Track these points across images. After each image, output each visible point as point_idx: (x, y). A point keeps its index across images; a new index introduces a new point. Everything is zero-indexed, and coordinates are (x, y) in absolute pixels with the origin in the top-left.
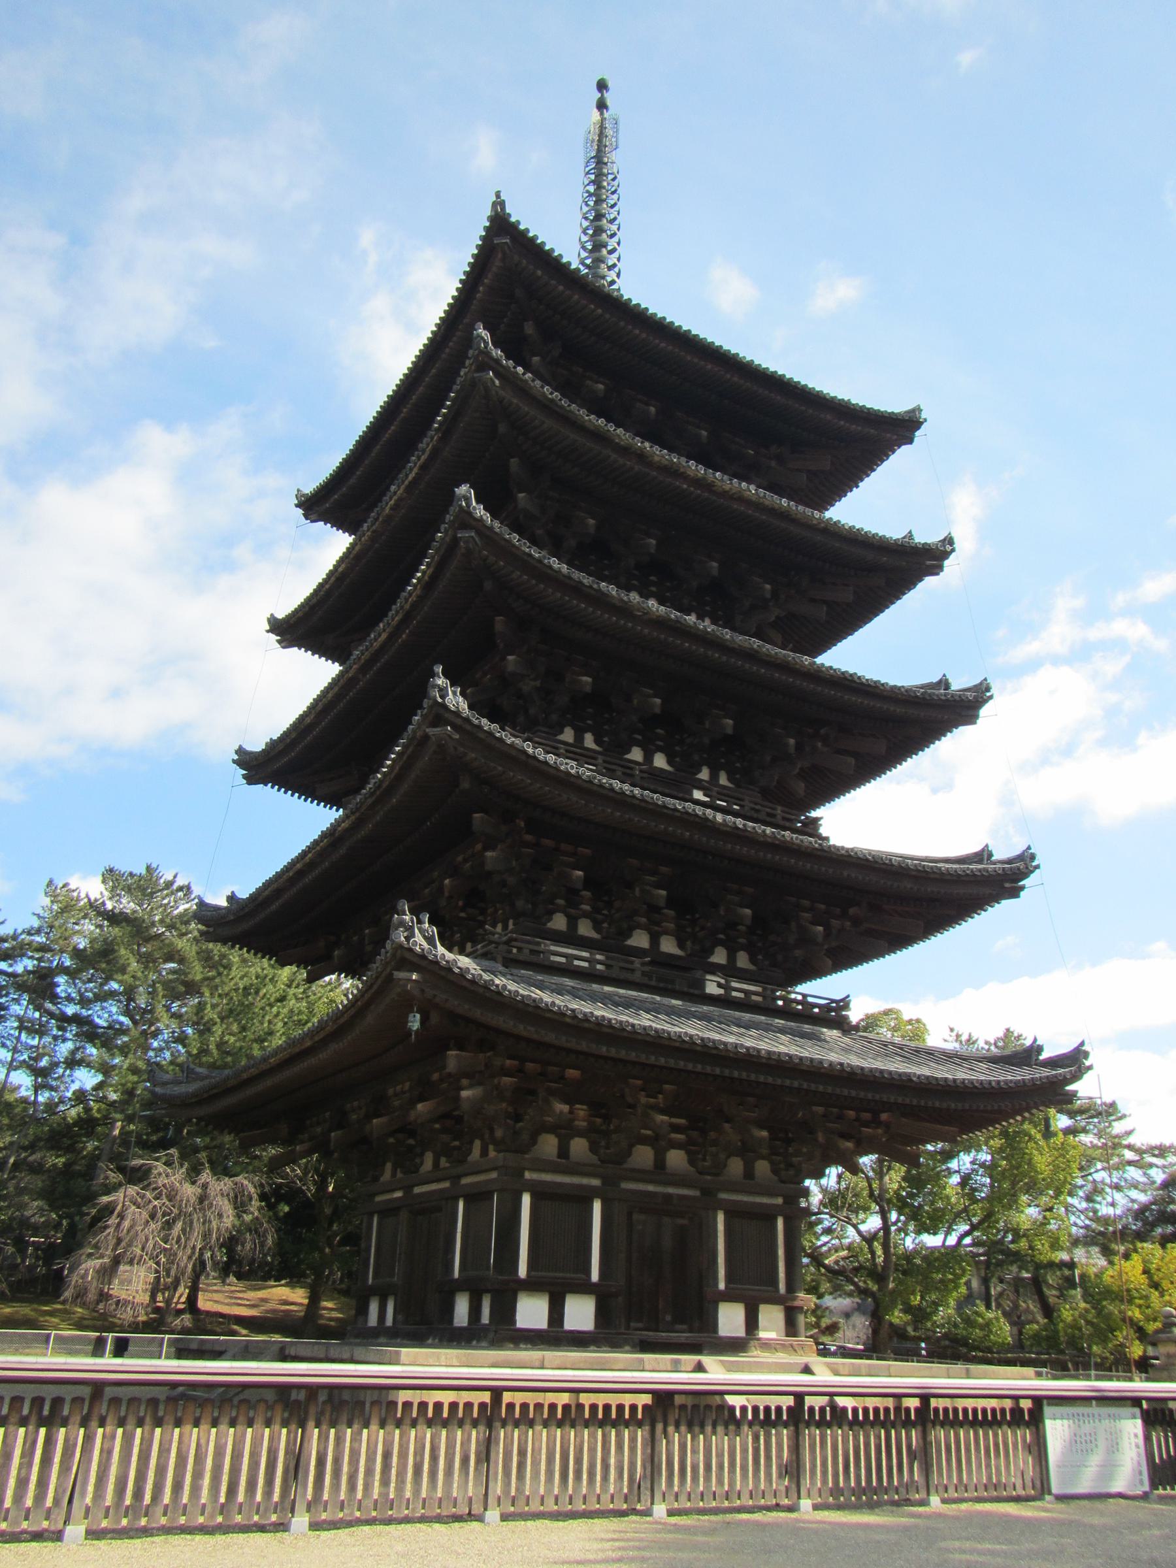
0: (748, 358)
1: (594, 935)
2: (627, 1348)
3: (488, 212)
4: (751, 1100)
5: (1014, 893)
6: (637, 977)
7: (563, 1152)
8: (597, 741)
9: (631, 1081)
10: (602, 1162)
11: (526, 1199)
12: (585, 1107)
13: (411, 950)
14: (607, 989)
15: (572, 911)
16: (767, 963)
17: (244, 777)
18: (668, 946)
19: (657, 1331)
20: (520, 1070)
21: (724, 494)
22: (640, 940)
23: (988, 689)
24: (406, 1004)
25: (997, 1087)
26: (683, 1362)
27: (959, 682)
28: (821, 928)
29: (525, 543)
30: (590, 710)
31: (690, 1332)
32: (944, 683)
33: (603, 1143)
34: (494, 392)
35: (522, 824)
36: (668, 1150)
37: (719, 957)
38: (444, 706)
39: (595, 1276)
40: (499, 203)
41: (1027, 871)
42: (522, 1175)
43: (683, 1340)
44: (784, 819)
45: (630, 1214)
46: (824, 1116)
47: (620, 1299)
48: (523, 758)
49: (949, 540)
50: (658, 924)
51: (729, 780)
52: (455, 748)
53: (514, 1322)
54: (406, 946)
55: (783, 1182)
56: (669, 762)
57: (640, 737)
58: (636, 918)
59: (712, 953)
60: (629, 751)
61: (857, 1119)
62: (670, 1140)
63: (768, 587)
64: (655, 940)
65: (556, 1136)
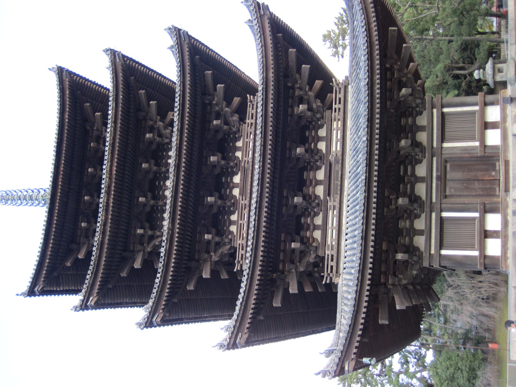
0: (53, 166)
1: (321, 215)
2: (508, 199)
3: (28, 297)
4: (387, 144)
5: (266, 8)
6: (337, 204)
7: (421, 233)
9: (385, 214)
10: (423, 213)
11: (444, 252)
12: (400, 221)
13: (335, 372)
15: (311, 228)
16: (322, 121)
18: (321, 175)
19: (499, 180)
20: (385, 274)
21: (110, 178)
22: (320, 191)
23: (170, 29)
25: (365, 27)
26: (514, 209)
27: (170, 41)
28: (301, 106)
29: (152, 296)
30: (220, 217)
31: (498, 160)
32: (172, 47)
33: (415, 212)
34: (95, 299)
35: (275, 275)
36: (416, 175)
37: (322, 146)
39: (476, 215)
41: (253, 4)
42: (433, 254)
43: (503, 167)
44: (252, 118)
45: (446, 197)
46: (391, 100)
47: (486, 203)
48: (244, 303)
49: (106, 51)
50: (311, 182)
51: (239, 141)
52: (246, 333)
53: (498, 256)
54: (334, 374)
55: (425, 109)
56: (237, 174)
58: (310, 193)
59: (321, 150)
60: (235, 196)
61: (391, 80)
62: (411, 176)
63: (148, 135)
64: (319, 183)
65: (414, 236)
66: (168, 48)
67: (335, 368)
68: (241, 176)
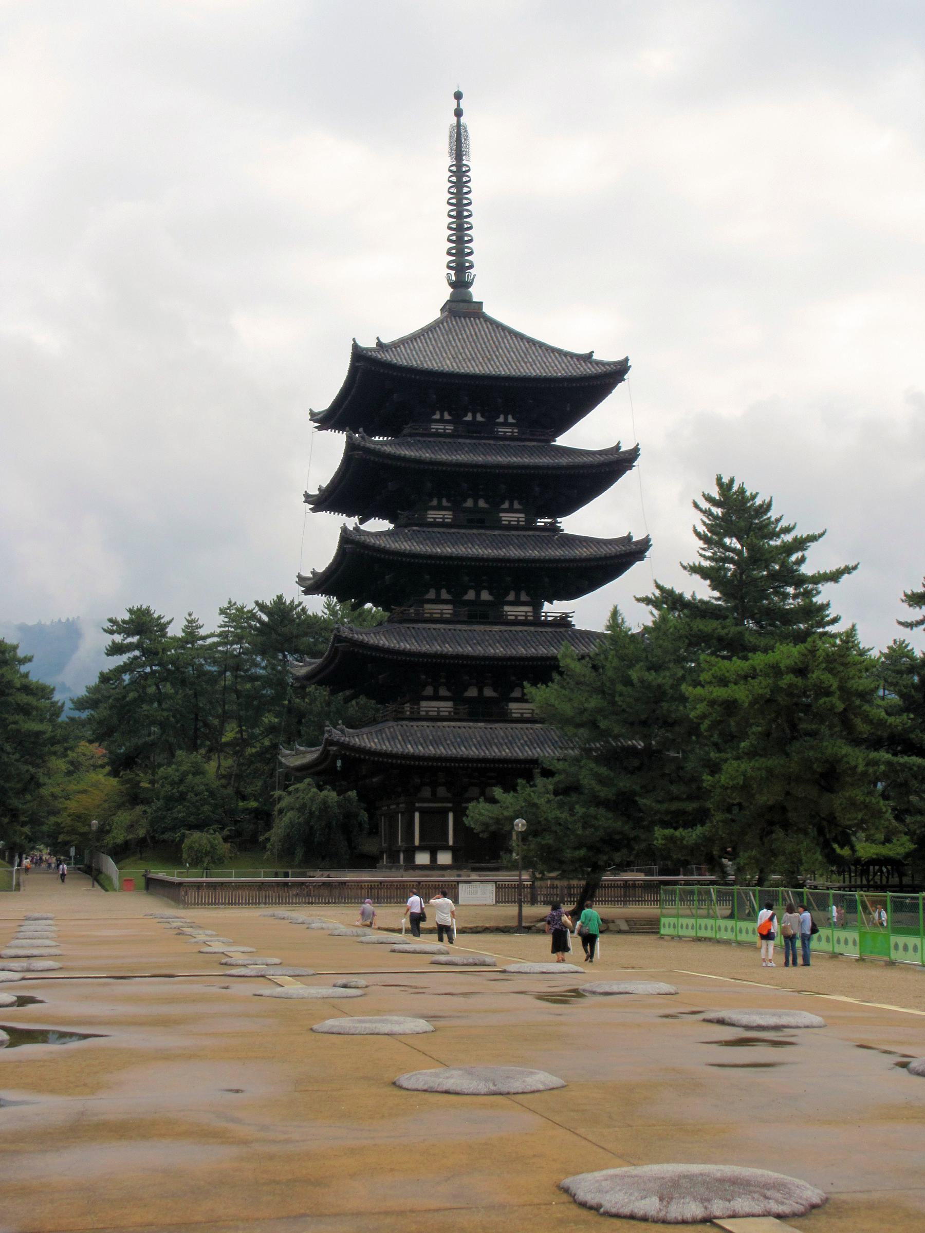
1: (448, 694)
7: (434, 793)
8: (449, 592)
11: (417, 815)
14: (445, 724)
17: (303, 591)
18: (489, 692)
22: (472, 692)
24: (336, 757)
32: (629, 538)
38: (341, 636)
39: (451, 843)
40: (355, 346)
51: (528, 594)
53: (414, 862)
56: (491, 594)
57: (473, 584)
59: (512, 691)
60: (466, 593)
64: (480, 691)
66: (630, 533)
67: (335, 740)
68: (488, 601)
